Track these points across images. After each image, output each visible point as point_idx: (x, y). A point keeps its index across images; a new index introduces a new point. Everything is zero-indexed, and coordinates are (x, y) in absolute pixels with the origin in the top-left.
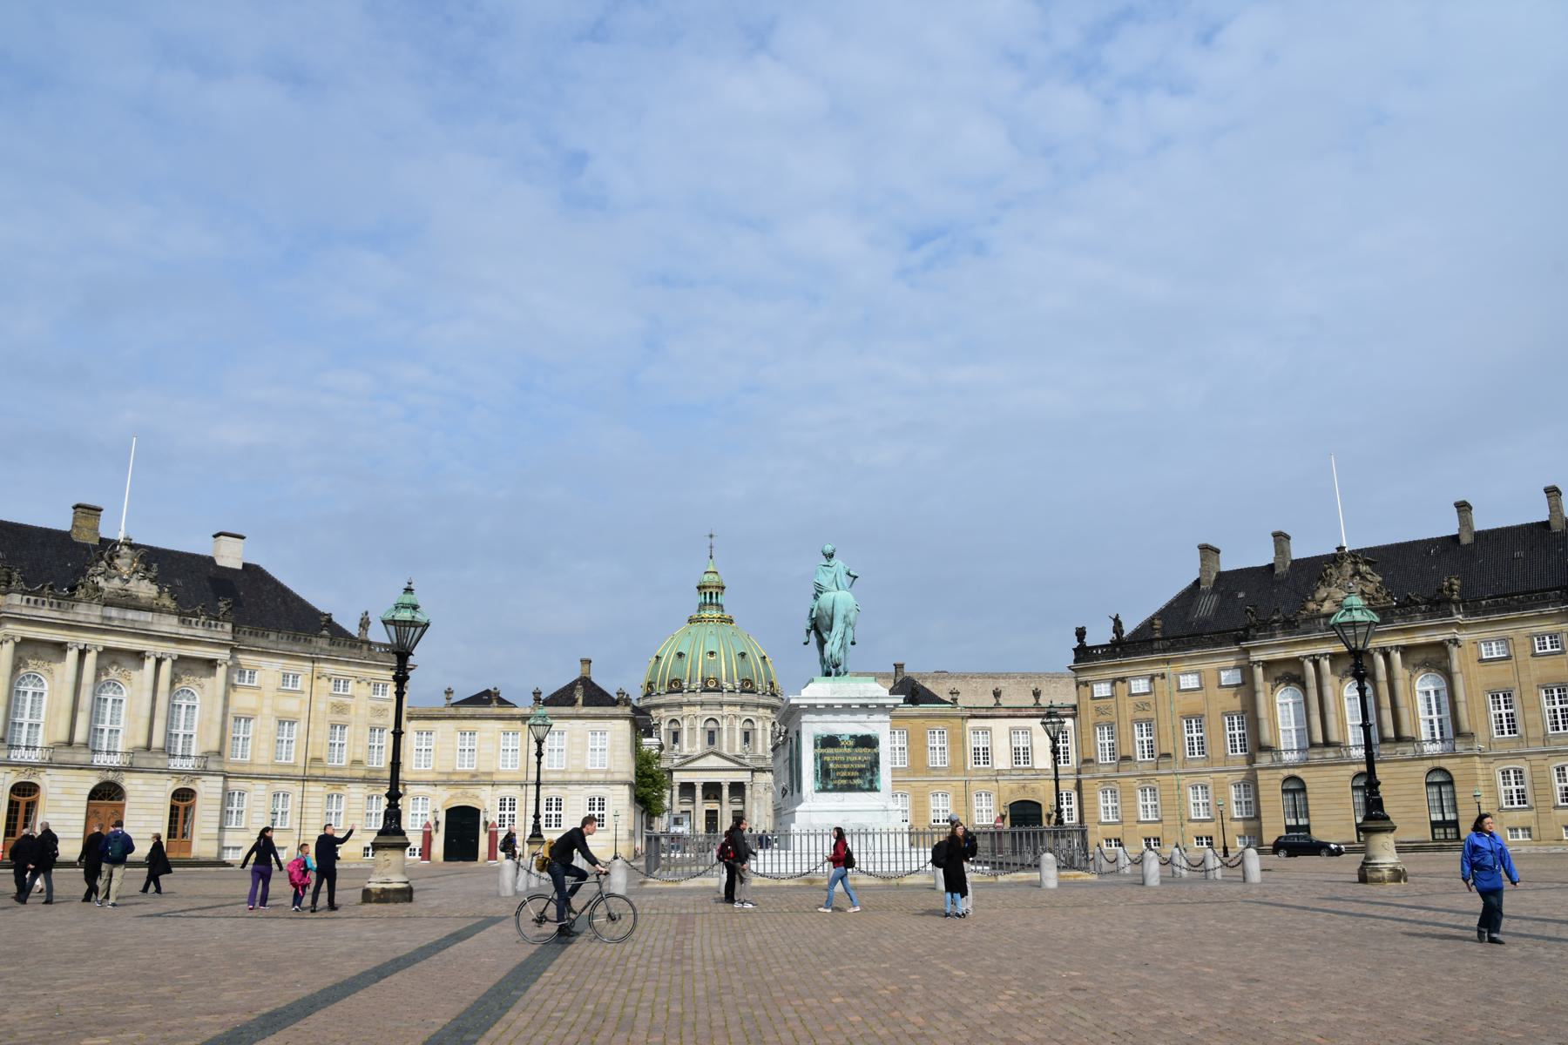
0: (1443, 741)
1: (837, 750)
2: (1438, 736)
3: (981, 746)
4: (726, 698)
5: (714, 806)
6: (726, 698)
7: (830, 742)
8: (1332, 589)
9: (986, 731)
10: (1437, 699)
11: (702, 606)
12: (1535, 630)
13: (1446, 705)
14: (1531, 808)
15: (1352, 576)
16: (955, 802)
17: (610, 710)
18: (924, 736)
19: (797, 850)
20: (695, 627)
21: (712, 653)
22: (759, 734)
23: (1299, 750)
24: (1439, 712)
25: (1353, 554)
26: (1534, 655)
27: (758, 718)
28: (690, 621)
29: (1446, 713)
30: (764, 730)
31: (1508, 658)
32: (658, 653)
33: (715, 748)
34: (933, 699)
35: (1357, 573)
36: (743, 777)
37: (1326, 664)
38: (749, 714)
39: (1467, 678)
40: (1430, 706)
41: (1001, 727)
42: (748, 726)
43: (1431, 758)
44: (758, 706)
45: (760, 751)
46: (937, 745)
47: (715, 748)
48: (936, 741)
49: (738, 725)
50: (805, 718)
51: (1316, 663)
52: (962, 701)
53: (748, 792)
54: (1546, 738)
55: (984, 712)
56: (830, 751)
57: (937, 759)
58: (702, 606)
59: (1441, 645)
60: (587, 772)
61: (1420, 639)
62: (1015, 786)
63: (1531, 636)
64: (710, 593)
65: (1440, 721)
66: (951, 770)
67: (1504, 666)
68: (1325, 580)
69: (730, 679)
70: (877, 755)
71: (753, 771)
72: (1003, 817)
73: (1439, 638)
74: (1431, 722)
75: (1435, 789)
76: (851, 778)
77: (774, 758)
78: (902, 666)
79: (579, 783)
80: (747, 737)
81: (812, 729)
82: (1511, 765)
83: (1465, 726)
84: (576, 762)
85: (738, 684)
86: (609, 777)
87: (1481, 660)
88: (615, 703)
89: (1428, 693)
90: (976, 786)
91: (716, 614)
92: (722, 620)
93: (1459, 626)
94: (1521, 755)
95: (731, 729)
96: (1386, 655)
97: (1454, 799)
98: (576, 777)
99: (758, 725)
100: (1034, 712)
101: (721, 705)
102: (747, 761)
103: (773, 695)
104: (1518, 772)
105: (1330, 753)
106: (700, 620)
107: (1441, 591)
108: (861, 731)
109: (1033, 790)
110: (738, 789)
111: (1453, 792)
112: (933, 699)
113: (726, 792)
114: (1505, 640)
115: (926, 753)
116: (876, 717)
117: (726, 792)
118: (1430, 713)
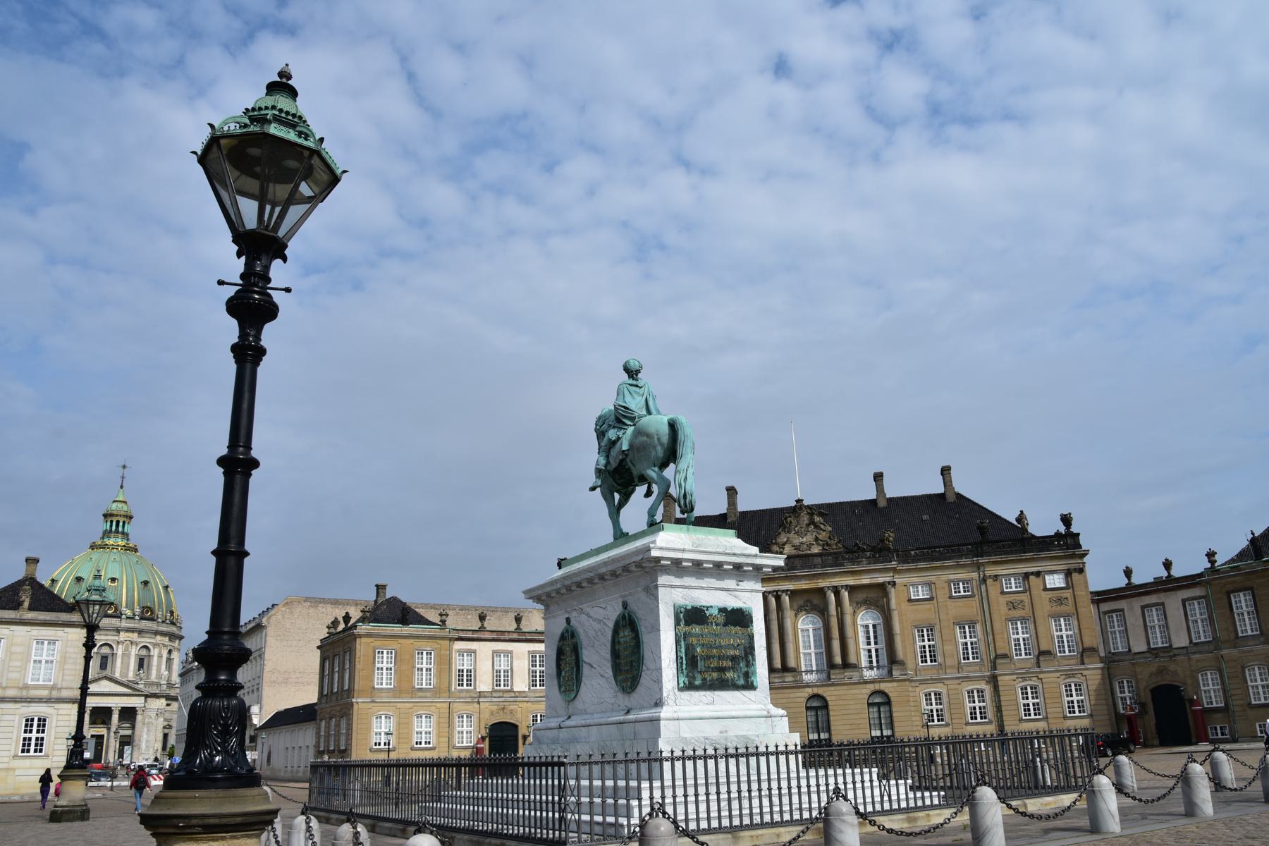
0: (878, 667)
1: (706, 630)
2: (875, 664)
3: (465, 668)
4: (125, 624)
5: (102, 731)
6: (125, 624)
7: (692, 616)
8: (792, 535)
9: (472, 652)
10: (875, 632)
11: (107, 534)
12: (952, 577)
13: (882, 638)
14: (947, 725)
15: (808, 525)
16: (439, 723)
17: (64, 617)
18: (413, 657)
19: (668, 783)
20: (96, 554)
21: (113, 580)
22: (155, 660)
23: (817, 671)
24: (876, 643)
25: (809, 507)
26: (951, 597)
27: (155, 645)
28: (93, 547)
29: (882, 645)
30: (160, 656)
31: (931, 599)
32: (54, 576)
33: (107, 672)
34: (423, 621)
35: (812, 522)
36: (136, 702)
37: (786, 599)
38: (146, 640)
39: (900, 615)
40: (868, 638)
41: (484, 649)
42: (144, 652)
43: (873, 682)
44: (156, 633)
45: (153, 677)
46: (424, 666)
47: (107, 672)
48: (424, 663)
49: (134, 651)
50: (662, 579)
51: (778, 598)
52: (451, 622)
53: (139, 718)
54: (959, 667)
55: (470, 635)
56: (696, 629)
57: (423, 680)
58: (107, 534)
59: (882, 587)
60: (26, 687)
61: (866, 580)
62: (495, 708)
63: (949, 582)
64: (116, 522)
65: (877, 650)
66: (436, 691)
67: (927, 606)
68: (785, 527)
69: (130, 605)
70: (751, 637)
71: (146, 696)
72: (483, 738)
73: (881, 580)
74: (870, 651)
75: (876, 709)
76: (722, 670)
77: (182, 683)
78: (384, 587)
79: (14, 700)
80: (141, 663)
81: (673, 595)
82: (932, 689)
83: (900, 655)
84: (14, 675)
85: (138, 610)
86: (55, 694)
87: (910, 600)
88: (70, 608)
89: (867, 626)
90: (459, 708)
91: (121, 542)
92: (126, 548)
93: (894, 570)
94: (940, 680)
95: (126, 655)
96: (837, 591)
97: (891, 717)
98: (11, 693)
99: (155, 652)
100: (515, 636)
101: (118, 630)
102: (141, 686)
103: (173, 623)
104: (938, 694)
105: (789, 678)
106: (104, 546)
107: (882, 541)
108: (732, 603)
109: (512, 712)
110: (129, 714)
111: (891, 711)
112: (423, 621)
113: (115, 717)
114: (929, 584)
115: (413, 674)
116: (747, 585)
117: (115, 717)
118: (869, 643)
